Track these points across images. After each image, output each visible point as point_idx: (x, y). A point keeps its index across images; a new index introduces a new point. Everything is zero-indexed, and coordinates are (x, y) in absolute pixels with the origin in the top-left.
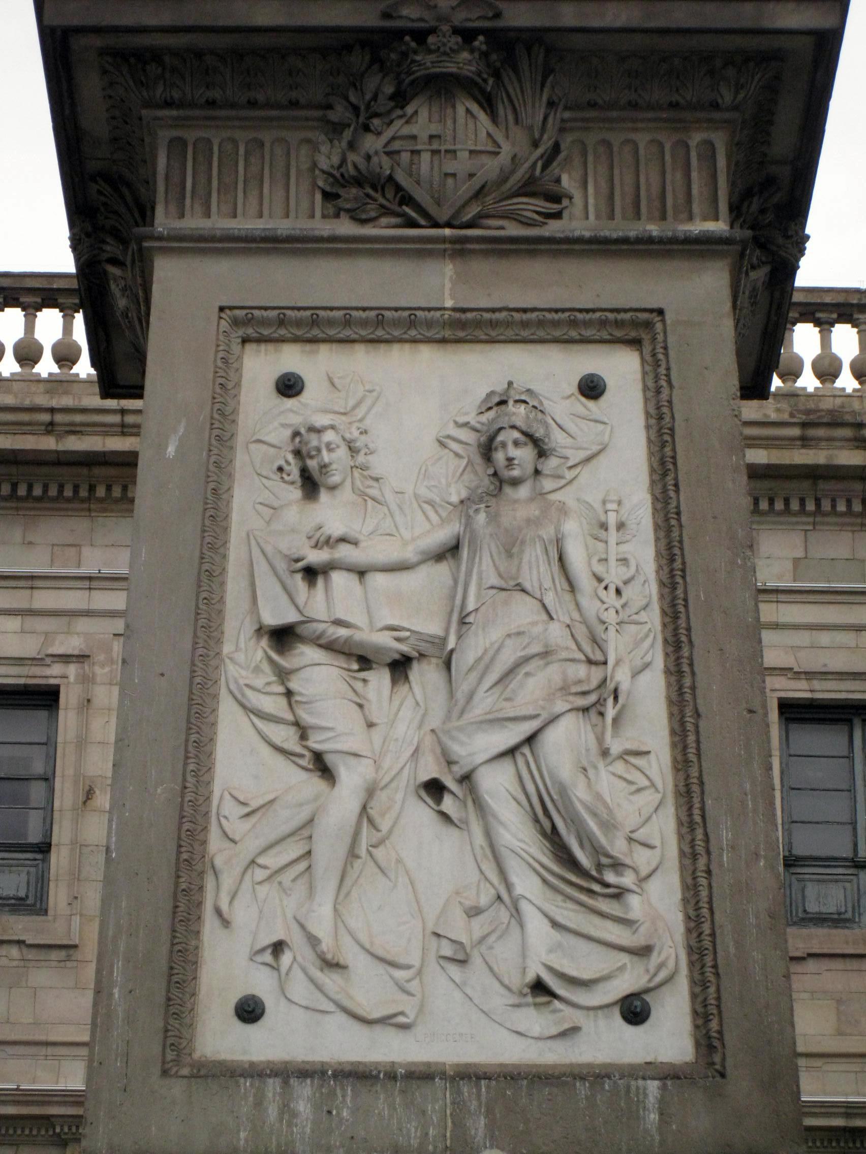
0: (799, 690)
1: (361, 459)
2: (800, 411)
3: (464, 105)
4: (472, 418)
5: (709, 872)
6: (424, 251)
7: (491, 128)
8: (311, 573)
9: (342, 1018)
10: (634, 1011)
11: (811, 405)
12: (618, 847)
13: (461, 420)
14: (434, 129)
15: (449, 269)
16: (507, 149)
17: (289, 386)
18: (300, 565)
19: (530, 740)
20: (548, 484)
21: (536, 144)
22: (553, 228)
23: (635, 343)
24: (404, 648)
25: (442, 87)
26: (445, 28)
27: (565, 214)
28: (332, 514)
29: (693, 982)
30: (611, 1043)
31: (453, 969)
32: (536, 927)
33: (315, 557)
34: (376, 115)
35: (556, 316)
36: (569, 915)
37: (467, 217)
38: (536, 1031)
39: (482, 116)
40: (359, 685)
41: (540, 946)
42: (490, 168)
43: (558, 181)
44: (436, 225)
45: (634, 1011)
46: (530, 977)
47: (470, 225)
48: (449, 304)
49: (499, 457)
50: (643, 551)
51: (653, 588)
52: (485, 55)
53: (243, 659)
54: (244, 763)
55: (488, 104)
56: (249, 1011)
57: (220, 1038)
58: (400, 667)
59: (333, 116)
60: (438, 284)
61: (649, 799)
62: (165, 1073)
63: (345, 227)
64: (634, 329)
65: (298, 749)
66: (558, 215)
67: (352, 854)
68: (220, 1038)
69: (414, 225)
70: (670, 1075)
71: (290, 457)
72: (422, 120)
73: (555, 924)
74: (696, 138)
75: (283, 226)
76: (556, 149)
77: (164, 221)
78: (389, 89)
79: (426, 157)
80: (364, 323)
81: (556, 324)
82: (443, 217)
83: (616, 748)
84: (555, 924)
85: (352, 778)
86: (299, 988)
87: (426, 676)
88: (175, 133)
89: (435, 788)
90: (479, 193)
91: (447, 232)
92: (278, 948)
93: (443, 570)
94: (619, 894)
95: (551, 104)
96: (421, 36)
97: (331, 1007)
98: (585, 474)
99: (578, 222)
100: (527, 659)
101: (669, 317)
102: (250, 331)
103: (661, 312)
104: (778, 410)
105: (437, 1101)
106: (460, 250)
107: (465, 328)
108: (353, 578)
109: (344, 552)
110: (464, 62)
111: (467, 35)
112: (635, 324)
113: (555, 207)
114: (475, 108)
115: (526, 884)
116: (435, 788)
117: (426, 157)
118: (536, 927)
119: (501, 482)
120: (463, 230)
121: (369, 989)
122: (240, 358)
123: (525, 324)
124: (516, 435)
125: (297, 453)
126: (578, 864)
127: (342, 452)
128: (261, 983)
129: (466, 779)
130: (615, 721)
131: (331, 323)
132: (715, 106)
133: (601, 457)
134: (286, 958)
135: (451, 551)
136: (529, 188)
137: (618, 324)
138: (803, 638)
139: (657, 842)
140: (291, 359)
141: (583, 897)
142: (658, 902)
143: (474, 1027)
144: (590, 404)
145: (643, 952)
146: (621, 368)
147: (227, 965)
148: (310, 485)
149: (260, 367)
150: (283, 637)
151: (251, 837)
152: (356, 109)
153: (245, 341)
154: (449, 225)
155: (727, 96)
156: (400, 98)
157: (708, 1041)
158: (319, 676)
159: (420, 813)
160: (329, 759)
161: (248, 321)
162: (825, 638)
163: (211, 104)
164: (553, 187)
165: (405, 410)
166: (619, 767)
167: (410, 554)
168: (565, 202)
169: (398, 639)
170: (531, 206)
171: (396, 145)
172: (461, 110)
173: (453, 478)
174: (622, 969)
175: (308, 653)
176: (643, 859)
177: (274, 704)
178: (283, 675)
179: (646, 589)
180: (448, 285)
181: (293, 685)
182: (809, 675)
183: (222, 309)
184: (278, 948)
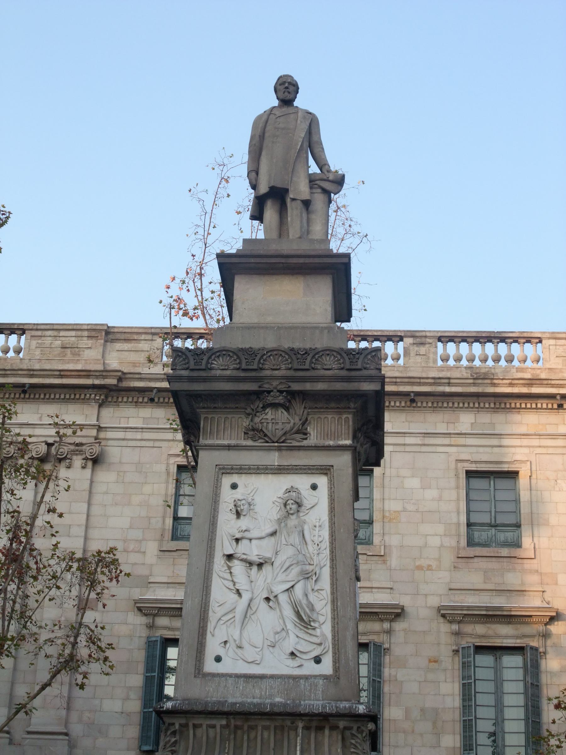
0: (473, 467)
1: (252, 507)
2: (474, 373)
3: (281, 411)
4: (281, 496)
5: (338, 623)
6: (269, 449)
7: (288, 416)
8: (237, 540)
9: (241, 661)
10: (318, 660)
11: (478, 371)
12: (314, 616)
13: (279, 496)
14: (273, 417)
15: (277, 454)
16: (292, 421)
18: (235, 538)
19: (292, 587)
20: (301, 514)
21: (300, 420)
22: (305, 443)
23: (326, 474)
24: (261, 561)
25: (275, 406)
26: (275, 390)
27: (308, 438)
28: (244, 523)
29: (333, 653)
30: (311, 669)
31: (271, 648)
32: (292, 637)
33: (238, 536)
34: (258, 412)
35: (305, 467)
36: (302, 635)
37: (281, 441)
38: (292, 665)
39: (285, 413)
40: (249, 570)
42: (288, 427)
43: (307, 429)
44: (274, 442)
45: (318, 660)
46: (290, 651)
47: (283, 442)
48: (276, 464)
49: (288, 507)
50: (326, 533)
51: (328, 544)
52: (285, 397)
53: (219, 562)
54: (220, 592)
55: (287, 409)
56: (218, 659)
57: (210, 666)
58: (260, 565)
59: (247, 412)
60: (274, 458)
61: (324, 602)
62: (195, 677)
63: (250, 443)
64: (325, 470)
65: (233, 588)
66: (306, 439)
67: (245, 616)
68: (210, 666)
69: (267, 442)
70: (325, 677)
71: (233, 507)
72: (270, 414)
73: (297, 637)
74: (344, 416)
75: (233, 442)
76: (307, 419)
77: (202, 441)
78: (261, 406)
79: (270, 424)
80: (254, 469)
81: (305, 469)
82: (275, 440)
83: (316, 589)
84: (297, 637)
85: (246, 596)
86: (231, 653)
87: (267, 569)
88: (206, 416)
89: (268, 599)
90: (285, 434)
91: (276, 444)
92: (226, 642)
93: (273, 539)
94: (314, 629)
95: (305, 408)
96: (269, 392)
97: (239, 658)
98: (311, 512)
99: (312, 440)
100: (292, 565)
101: (335, 468)
102: (224, 471)
103: (332, 466)
104: (467, 373)
105: (265, 684)
106: (279, 449)
107: (280, 470)
108: (249, 541)
109: (247, 535)
110: (280, 399)
111: (281, 392)
112: (326, 469)
113: (305, 437)
114: (284, 411)
115: (290, 626)
116: (268, 599)
117: (270, 424)
118: (292, 637)
119: (289, 514)
120: (281, 443)
121: (250, 653)
122: (221, 479)
123: (297, 469)
124: (292, 501)
125: (235, 505)
126: (305, 621)
127: (246, 506)
128: (221, 652)
129: (276, 597)
130: (316, 581)
131: (245, 469)
132: (349, 408)
133: (316, 507)
134: (228, 645)
135: (274, 534)
136: (298, 432)
137: (321, 469)
138: (474, 449)
139: (325, 614)
140: (235, 478)
141: (305, 630)
144: (314, 492)
145: (320, 644)
146: (322, 481)
147: (213, 646)
148: (238, 514)
149: (227, 481)
150: (230, 557)
151: (220, 611)
152: (253, 410)
153: (223, 473)
154: (277, 442)
155: (352, 405)
156: (264, 408)
157: (336, 669)
158: (238, 567)
159: (264, 605)
160: (240, 591)
161: (224, 468)
162: (481, 450)
163: (215, 408)
164: (305, 431)
165: (265, 493)
166: (316, 594)
167: (263, 534)
168: (308, 435)
169: (259, 558)
171: (263, 421)
172: (280, 412)
173: (275, 513)
174: (314, 649)
175: (236, 562)
176: (322, 619)
177: (228, 576)
178: (229, 568)
179: (326, 544)
180: (276, 459)
181: (232, 571)
182: (476, 462)
183: (216, 465)
184: (226, 642)
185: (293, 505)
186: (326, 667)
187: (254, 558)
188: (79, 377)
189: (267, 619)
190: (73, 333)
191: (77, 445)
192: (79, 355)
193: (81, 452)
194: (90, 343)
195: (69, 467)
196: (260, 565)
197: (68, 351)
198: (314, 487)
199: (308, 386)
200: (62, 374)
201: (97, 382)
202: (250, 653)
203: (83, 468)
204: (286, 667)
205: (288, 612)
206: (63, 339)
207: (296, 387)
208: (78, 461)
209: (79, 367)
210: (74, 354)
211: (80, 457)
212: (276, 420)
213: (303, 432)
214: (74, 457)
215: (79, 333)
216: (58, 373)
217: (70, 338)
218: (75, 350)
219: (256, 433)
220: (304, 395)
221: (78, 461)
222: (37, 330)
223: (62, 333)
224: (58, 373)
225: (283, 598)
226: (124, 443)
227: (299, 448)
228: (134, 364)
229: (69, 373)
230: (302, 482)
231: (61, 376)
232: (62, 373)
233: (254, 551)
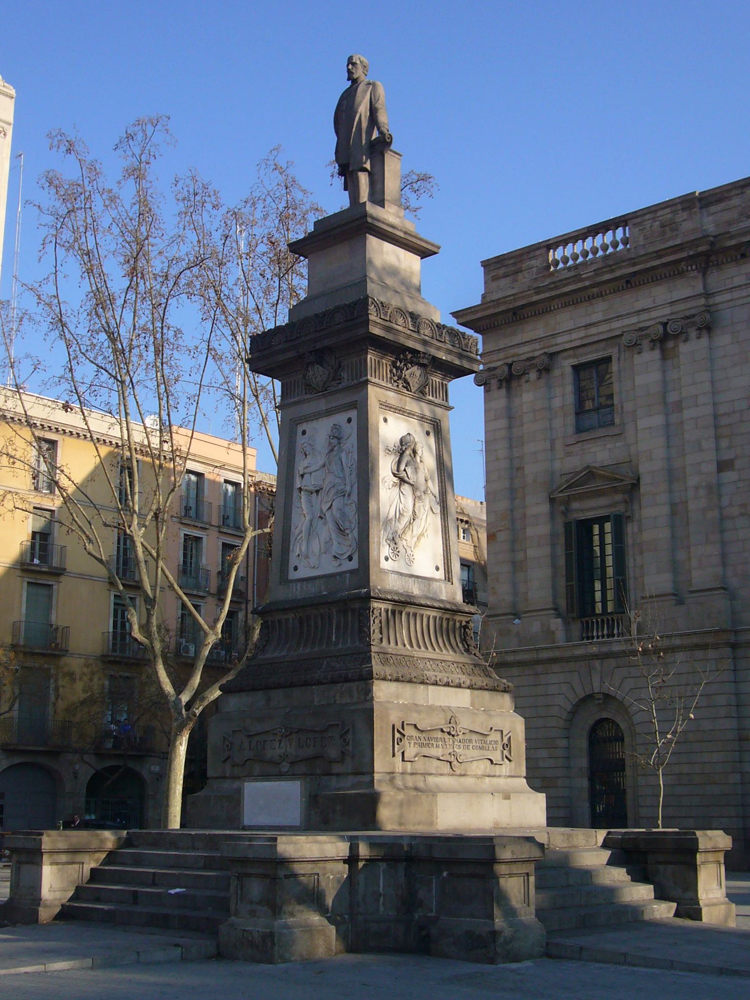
17: (304, 433)
23: (356, 408)
41: (335, 549)
45: (350, 558)
56: (296, 568)
57: (293, 575)
58: (317, 492)
60: (322, 405)
63: (308, 396)
68: (293, 575)
90: (325, 383)
95: (336, 358)
99: (344, 384)
106: (325, 396)
107: (329, 413)
115: (334, 536)
120: (324, 390)
121: (313, 561)
126: (341, 531)
136: (334, 379)
147: (293, 561)
150: (300, 489)
167: (318, 468)
170: (334, 383)
187: (311, 488)
188: (675, 252)
190: (668, 210)
191: (688, 318)
192: (677, 230)
193: (694, 324)
194: (685, 215)
195: (686, 340)
196: (317, 492)
197: (667, 228)
198: (349, 420)
199: (326, 343)
200: (659, 254)
201: (691, 253)
202: (313, 561)
203: (699, 338)
206: (660, 218)
207: (318, 346)
208: (693, 334)
209: (678, 241)
210: (672, 230)
211: (694, 328)
213: (337, 378)
214: (689, 330)
215: (673, 208)
216: (655, 255)
217: (666, 215)
218: (670, 226)
219: (309, 388)
221: (693, 334)
222: (637, 217)
223: (659, 213)
224: (655, 255)
226: (731, 304)
227: (336, 392)
228: (729, 223)
229: (664, 252)
230: (340, 418)
231: (660, 257)
232: (659, 253)
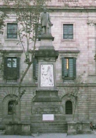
0: (64, 23)
10: (52, 85)
25: (47, 57)
28: (44, 70)
30: (52, 86)
45: (52, 85)
53: (41, 75)
64: (52, 64)
68: (41, 86)
72: (46, 58)
107: (48, 64)
121: (45, 84)
126: (51, 81)
138: (65, 20)
140: (43, 65)
142: (53, 82)
143: (48, 85)
146: (52, 65)
147: (41, 84)
148: (43, 69)
149: (42, 65)
150: (43, 74)
158: (43, 75)
173: (47, 69)
185: (49, 68)
186: (53, 86)
189: (47, 81)
199: (50, 55)
202: (45, 84)
204: (49, 86)
205: (49, 80)
212: (47, 59)
213: (50, 60)
219: (45, 60)
220: (50, 56)
225: (49, 79)
230: (50, 65)
233: (45, 73)
